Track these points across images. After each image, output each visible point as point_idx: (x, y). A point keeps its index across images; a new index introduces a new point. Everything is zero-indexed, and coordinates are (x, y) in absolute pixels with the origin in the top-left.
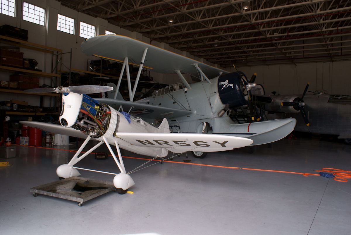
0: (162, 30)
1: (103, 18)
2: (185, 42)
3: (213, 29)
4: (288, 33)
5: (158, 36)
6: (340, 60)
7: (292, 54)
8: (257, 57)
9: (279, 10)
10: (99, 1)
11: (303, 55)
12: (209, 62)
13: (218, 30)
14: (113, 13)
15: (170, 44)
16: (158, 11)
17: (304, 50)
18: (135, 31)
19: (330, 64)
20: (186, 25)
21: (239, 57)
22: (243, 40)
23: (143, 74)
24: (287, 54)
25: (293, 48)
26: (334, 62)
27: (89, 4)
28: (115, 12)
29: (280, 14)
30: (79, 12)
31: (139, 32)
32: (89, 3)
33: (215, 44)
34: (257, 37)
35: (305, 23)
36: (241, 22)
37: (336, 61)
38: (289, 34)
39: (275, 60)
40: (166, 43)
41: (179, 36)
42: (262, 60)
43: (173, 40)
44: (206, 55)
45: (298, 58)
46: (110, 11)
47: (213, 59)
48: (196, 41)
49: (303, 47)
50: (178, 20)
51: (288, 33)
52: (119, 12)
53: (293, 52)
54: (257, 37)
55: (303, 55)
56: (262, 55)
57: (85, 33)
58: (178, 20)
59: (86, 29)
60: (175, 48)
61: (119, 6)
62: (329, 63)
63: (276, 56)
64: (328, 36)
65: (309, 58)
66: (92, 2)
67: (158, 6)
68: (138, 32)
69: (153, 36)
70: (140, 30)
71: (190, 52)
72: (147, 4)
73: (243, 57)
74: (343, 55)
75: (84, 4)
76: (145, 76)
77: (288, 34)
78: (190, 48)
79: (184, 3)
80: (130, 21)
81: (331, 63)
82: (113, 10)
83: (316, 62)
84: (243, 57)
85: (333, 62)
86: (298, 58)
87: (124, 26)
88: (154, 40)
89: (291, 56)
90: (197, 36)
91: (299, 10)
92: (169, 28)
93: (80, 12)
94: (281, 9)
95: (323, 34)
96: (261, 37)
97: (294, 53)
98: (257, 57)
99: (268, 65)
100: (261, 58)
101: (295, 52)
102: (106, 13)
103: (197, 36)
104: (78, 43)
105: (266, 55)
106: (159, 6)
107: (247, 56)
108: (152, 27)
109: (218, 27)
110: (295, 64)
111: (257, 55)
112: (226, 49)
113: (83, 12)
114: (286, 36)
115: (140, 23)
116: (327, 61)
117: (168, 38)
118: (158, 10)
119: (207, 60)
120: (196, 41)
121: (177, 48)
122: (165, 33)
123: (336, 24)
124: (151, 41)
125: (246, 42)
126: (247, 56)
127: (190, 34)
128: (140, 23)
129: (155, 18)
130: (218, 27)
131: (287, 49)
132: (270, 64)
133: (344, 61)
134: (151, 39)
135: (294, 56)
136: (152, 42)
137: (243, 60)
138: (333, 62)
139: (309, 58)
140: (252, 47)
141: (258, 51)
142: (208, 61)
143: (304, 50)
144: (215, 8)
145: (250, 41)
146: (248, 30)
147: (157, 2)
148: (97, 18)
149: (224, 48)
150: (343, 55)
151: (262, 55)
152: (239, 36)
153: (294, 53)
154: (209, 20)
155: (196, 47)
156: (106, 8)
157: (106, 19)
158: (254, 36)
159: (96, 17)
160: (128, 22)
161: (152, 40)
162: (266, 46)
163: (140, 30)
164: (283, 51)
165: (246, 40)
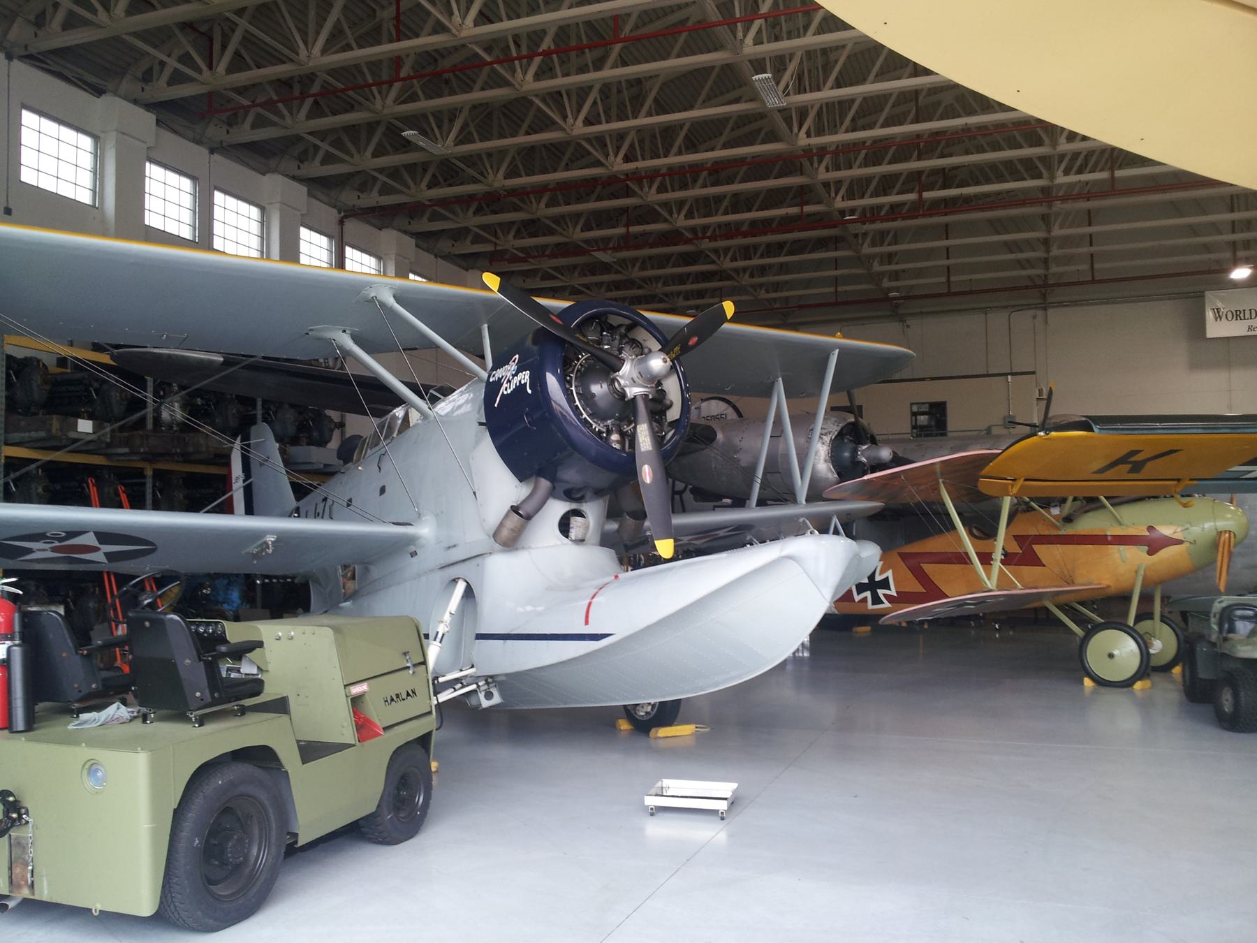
0: (394, 173)
1: (135, 102)
2: (485, 227)
4: (920, 193)
5: (373, 198)
6: (1074, 303)
8: (763, 295)
9: (878, 97)
10: (131, 11)
11: (948, 281)
14: (192, 80)
16: (539, 55)
17: (951, 262)
18: (275, 171)
19: (1035, 317)
20: (502, 152)
24: (885, 280)
26: (1051, 312)
27: (71, 22)
28: (200, 71)
29: (887, 110)
30: (16, 63)
31: (294, 178)
32: (71, 14)
34: (795, 210)
35: (951, 155)
36: (724, 147)
37: (1061, 304)
38: (1104, 175)
39: (836, 304)
40: (405, 232)
41: (465, 201)
42: (777, 305)
43: (434, 217)
45: (1066, 284)
46: (172, 63)
48: (532, 227)
49: (948, 252)
50: (473, 130)
51: (920, 193)
52: (220, 77)
54: (795, 210)
55: (948, 281)
56: (777, 287)
57: (48, 164)
58: (473, 130)
59: (49, 145)
61: (217, 47)
62: (1032, 312)
63: (839, 289)
65: (971, 292)
66: (94, 11)
67: (537, 35)
68: (287, 176)
69: (350, 197)
72: (354, 45)
74: (1100, 282)
75: (40, 21)
77: (921, 196)
79: (524, 51)
80: (259, 123)
81: (1040, 313)
82: (185, 59)
83: (984, 310)
85: (1045, 309)
86: (1066, 284)
87: (230, 146)
90: (542, 205)
91: (939, 103)
92: (425, 167)
93: (21, 58)
94: (853, 101)
96: (807, 209)
98: (763, 295)
100: (775, 300)
102: (147, 77)
103: (542, 205)
104: (14, 211)
106: (544, 32)
108: (356, 156)
109: (641, 164)
110: (902, 319)
112: (645, 263)
113: (36, 59)
114: (913, 202)
115: (310, 133)
116: (1028, 307)
117: (413, 210)
118: (403, 74)
120: (532, 227)
121: (447, 257)
122: (409, 188)
124: (341, 222)
128: (310, 133)
130: (641, 164)
138: (1045, 309)
139: (971, 292)
143: (951, 262)
144: (627, 81)
145: (745, 228)
146: (743, 181)
147: (534, 10)
148: (104, 97)
149: (637, 259)
150: (1100, 282)
151: (777, 287)
154: (610, 132)
155: (528, 254)
156: (155, 47)
157: (149, 107)
158: (761, 209)
159: (98, 92)
160: (247, 125)
161: (345, 217)
162: (821, 244)
164: (877, 267)
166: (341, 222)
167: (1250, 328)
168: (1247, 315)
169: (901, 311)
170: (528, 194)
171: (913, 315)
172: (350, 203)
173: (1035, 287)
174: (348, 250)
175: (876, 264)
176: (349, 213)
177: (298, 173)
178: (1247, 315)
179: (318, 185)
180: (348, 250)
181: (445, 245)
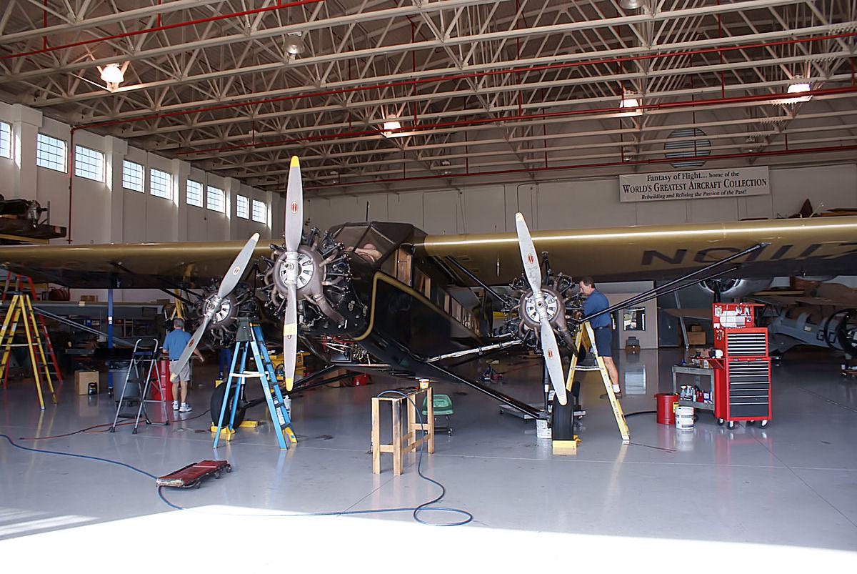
3: (229, 102)
5: (90, 118)
6: (549, 181)
7: (445, 165)
12: (250, 187)
13: (244, 105)
15: (132, 141)
19: (531, 189)
21: (321, 173)
22: (323, 131)
23: (36, 217)
25: (450, 151)
26: (539, 185)
31: (31, 106)
33: (249, 139)
37: (542, 181)
42: (377, 179)
44: (238, 170)
47: (259, 178)
53: (447, 160)
56: (379, 168)
60: (147, 151)
62: (530, 186)
64: (508, 125)
69: (77, 118)
70: (35, 100)
71: (192, 161)
73: (331, 173)
76: (45, 223)
78: (189, 151)
81: (534, 186)
84: (331, 173)
88: (82, 128)
89: (444, 170)
95: (499, 116)
97: (448, 163)
99: (396, 192)
100: (376, 176)
101: (452, 161)
105: (388, 167)
107: (342, 171)
111: (362, 168)
116: (525, 182)
117: (124, 124)
119: (244, 181)
123: (524, 96)
124: (72, 133)
125: (331, 135)
126: (342, 171)
127: (178, 114)
129: (62, 68)
131: (431, 152)
132: (399, 190)
133: (558, 182)
134: (71, 126)
135: (449, 170)
136: (77, 133)
137: (332, 179)
138: (537, 184)
140: (349, 147)
141: (365, 158)
142: (246, 184)
151: (379, 168)
152: (310, 120)
153: (448, 163)
154: (218, 79)
155: (205, 149)
161: (74, 129)
163: (35, 100)
165: (330, 131)
166: (72, 133)
167: (643, 197)
168: (642, 190)
169: (453, 184)
170: (183, 113)
171: (464, 186)
172: (77, 121)
173: (528, 170)
174: (78, 149)
175: (420, 156)
176: (77, 127)
177: (33, 103)
178: (642, 190)
179: (48, 110)
180: (78, 149)
181: (152, 144)
